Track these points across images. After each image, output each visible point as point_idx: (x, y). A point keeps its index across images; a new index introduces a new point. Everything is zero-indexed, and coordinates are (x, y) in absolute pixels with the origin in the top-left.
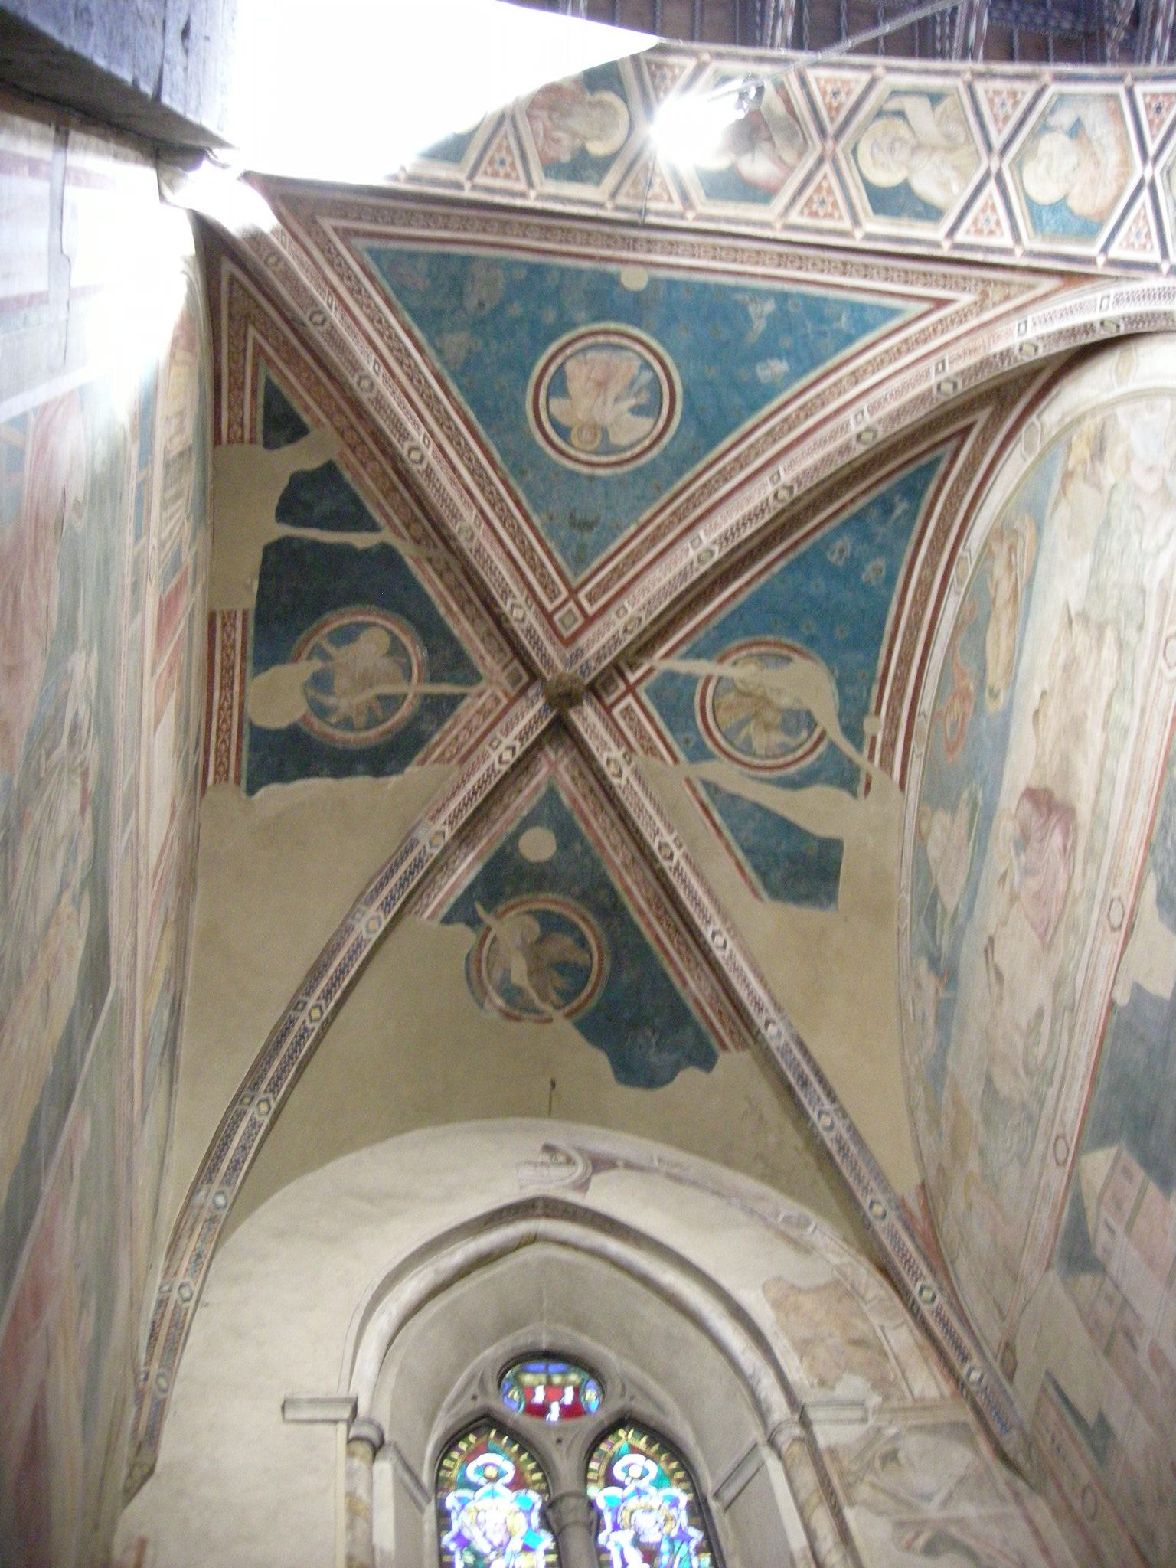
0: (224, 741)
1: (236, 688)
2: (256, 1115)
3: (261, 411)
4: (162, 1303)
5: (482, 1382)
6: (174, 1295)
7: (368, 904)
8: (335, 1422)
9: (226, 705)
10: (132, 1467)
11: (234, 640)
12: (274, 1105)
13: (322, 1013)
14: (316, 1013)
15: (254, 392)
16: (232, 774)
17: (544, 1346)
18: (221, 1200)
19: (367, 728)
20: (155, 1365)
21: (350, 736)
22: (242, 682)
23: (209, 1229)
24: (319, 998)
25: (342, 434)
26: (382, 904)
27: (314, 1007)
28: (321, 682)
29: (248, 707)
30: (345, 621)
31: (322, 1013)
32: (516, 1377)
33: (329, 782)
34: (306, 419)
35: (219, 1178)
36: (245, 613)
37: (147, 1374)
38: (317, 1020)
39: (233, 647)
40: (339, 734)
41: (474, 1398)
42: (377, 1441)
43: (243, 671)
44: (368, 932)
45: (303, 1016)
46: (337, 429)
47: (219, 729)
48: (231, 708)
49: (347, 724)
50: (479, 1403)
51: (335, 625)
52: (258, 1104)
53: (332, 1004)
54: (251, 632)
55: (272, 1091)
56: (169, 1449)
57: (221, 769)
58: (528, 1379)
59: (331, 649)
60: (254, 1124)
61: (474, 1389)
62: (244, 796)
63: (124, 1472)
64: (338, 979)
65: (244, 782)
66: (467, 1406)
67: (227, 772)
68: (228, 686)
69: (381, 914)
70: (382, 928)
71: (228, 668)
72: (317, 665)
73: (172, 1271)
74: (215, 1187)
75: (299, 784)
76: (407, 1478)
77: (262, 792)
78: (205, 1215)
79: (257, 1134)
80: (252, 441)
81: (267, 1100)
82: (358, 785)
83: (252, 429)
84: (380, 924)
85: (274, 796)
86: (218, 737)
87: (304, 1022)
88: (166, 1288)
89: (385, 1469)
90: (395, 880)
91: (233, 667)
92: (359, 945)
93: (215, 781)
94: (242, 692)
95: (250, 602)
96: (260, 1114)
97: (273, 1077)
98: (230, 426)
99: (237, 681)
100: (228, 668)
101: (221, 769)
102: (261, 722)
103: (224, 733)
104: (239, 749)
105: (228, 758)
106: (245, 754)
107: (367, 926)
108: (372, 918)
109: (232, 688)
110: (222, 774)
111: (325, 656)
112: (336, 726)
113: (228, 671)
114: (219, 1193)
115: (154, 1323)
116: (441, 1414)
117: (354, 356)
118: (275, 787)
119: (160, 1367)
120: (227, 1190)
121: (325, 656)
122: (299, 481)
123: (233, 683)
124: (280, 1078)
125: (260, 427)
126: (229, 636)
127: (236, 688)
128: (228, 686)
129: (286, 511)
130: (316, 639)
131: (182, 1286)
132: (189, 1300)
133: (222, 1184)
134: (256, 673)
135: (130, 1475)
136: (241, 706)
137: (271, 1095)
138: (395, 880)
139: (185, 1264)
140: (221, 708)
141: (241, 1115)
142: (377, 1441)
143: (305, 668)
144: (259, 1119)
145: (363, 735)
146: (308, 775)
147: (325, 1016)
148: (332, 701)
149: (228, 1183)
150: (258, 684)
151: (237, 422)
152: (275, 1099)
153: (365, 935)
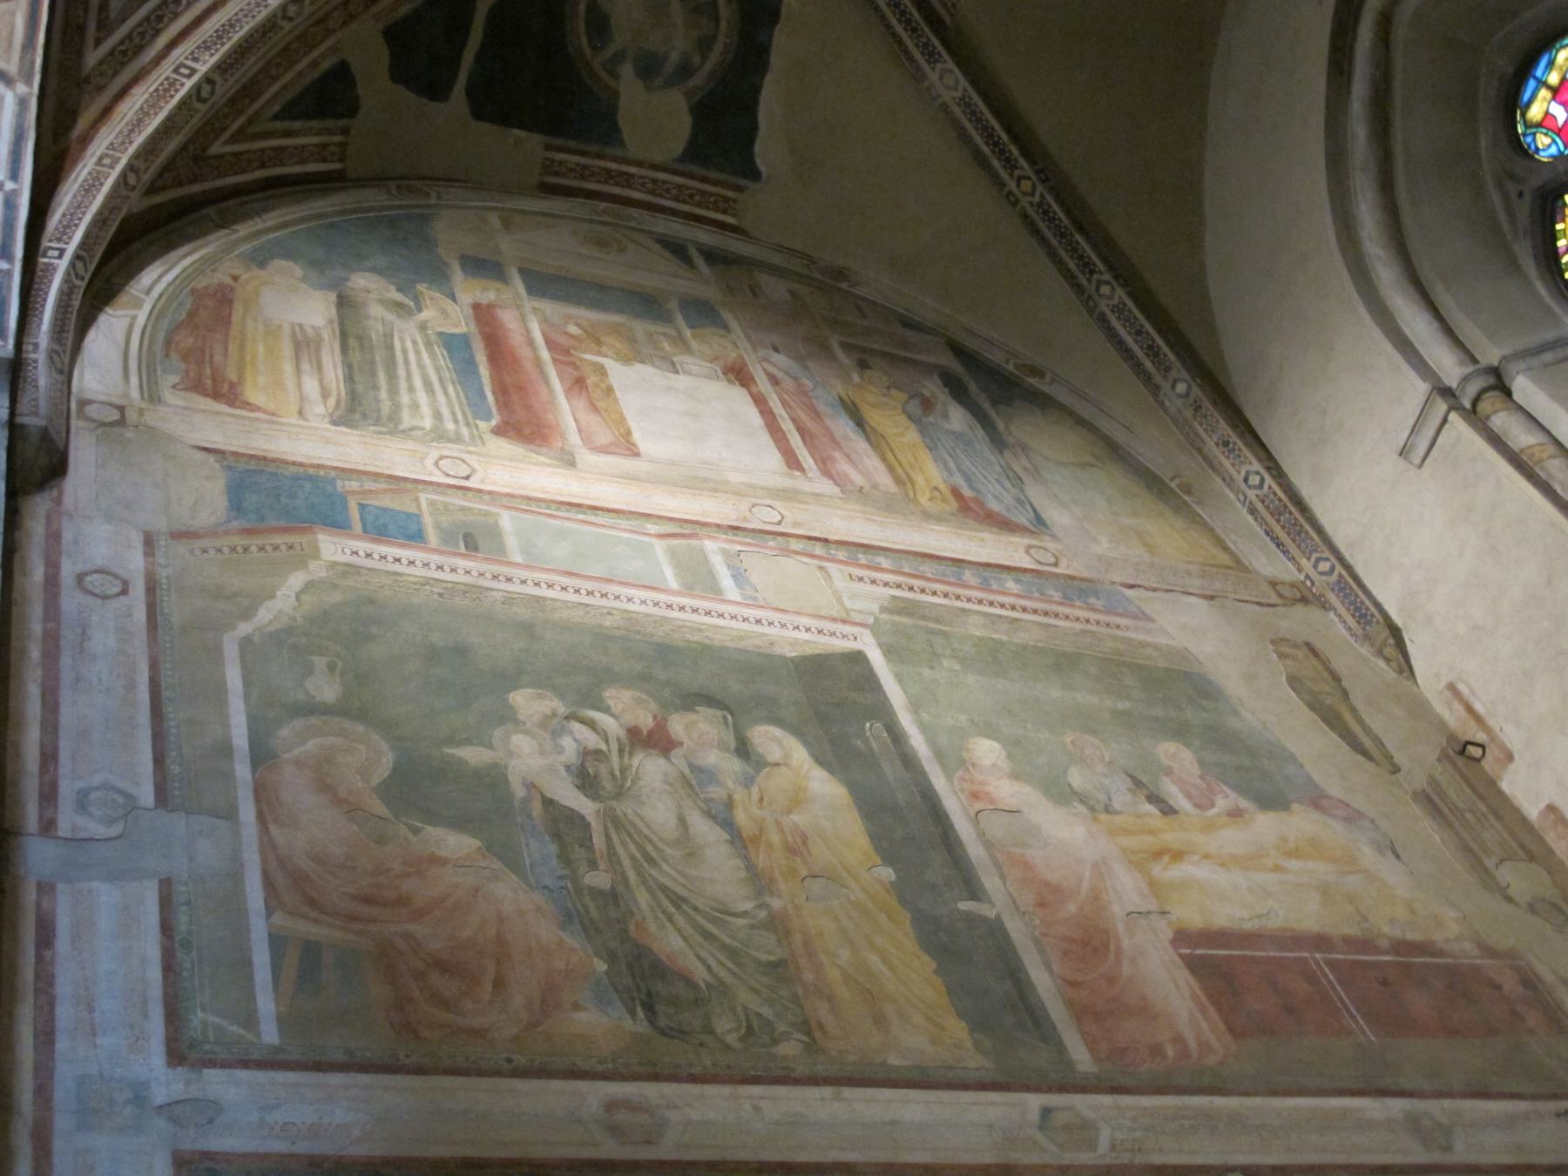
0: (691, 196)
1: (633, 170)
2: (1111, 302)
3: (314, 124)
4: (1253, 511)
5: (1511, 177)
6: (1252, 494)
7: (924, 77)
8: (1445, 421)
9: (650, 186)
10: (1380, 653)
11: (578, 165)
12: (1107, 277)
13: (1029, 178)
14: (1026, 185)
15: (288, 134)
16: (730, 194)
17: (1511, 70)
18: (1181, 388)
19: (717, 19)
20: (1304, 562)
21: (719, 47)
22: (628, 162)
23: (1205, 416)
24: (1011, 175)
25: (352, 17)
26: (928, 62)
27: (1018, 185)
28: (649, 68)
29: (658, 158)
30: (582, 27)
31: (1029, 178)
32: (1527, 125)
33: (769, 79)
34: (326, 65)
35: (1158, 379)
36: (548, 147)
37: (1307, 577)
38: (1034, 187)
39: (585, 167)
40: (715, 56)
41: (1521, 195)
42: (1491, 381)
43: (615, 159)
44: (956, 89)
45: (1025, 201)
46: (345, 23)
47: (677, 200)
48: (654, 181)
49: (705, 44)
50: (1527, 197)
51: (584, 40)
52: (1099, 294)
53: (1022, 162)
54: (572, 143)
55: (1092, 272)
56: (1389, 595)
57: (721, 205)
58: (1535, 112)
59: (612, 49)
60: (1119, 309)
61: (1511, 187)
62: (759, 186)
63: (1382, 664)
64: (996, 144)
65: (741, 182)
66: (1524, 208)
67: (727, 199)
68: (628, 181)
69: (939, 66)
70: (956, 71)
71: (609, 176)
72: (627, 70)
73: (1227, 478)
74: (1166, 386)
75: (762, 116)
76: (1548, 357)
77: (760, 163)
78: (1188, 413)
79: (1130, 311)
80: (345, 131)
81: (1099, 283)
82: (783, 46)
83: (330, 132)
84: (951, 71)
85: (768, 150)
86: (684, 202)
87: (1031, 204)
88: (1241, 497)
89: (1524, 387)
90: (904, 36)
91: (608, 171)
92: (965, 103)
93: (734, 215)
94: (639, 164)
95: (536, 140)
96: (1111, 297)
97: (1077, 265)
98: (325, 161)
99: (624, 168)
100: (609, 176)
101: (721, 205)
102: (679, 147)
103: (681, 194)
104: (704, 180)
105: (711, 194)
106: (714, 175)
107: (948, 88)
108: (941, 78)
109: (632, 176)
110: (727, 205)
111: (620, 56)
112: (704, 58)
113: (611, 177)
114: (1173, 387)
115: (1267, 533)
116: (1516, 247)
117: (257, 31)
118: (758, 147)
119: (1309, 559)
120: (1174, 374)
121: (620, 56)
122: (402, 72)
123: (626, 174)
124: (1081, 258)
125: (331, 123)
126: (571, 170)
127: (633, 170)
128: (628, 181)
129: (435, 90)
130: (596, 66)
131: (1246, 480)
132: (1262, 480)
133: (1165, 377)
134: (621, 143)
135: (1387, 660)
136: (654, 167)
137: (1096, 276)
138: (904, 36)
139: (1227, 464)
140: (652, 192)
141: (1103, 319)
142: (1491, 381)
143: (628, 84)
144: (1116, 301)
145: (723, 24)
146: (756, 103)
147: (1033, 177)
148: (674, 57)
149: (1168, 369)
150: (635, 139)
151: (321, 153)
152: (1100, 272)
153: (958, 94)
